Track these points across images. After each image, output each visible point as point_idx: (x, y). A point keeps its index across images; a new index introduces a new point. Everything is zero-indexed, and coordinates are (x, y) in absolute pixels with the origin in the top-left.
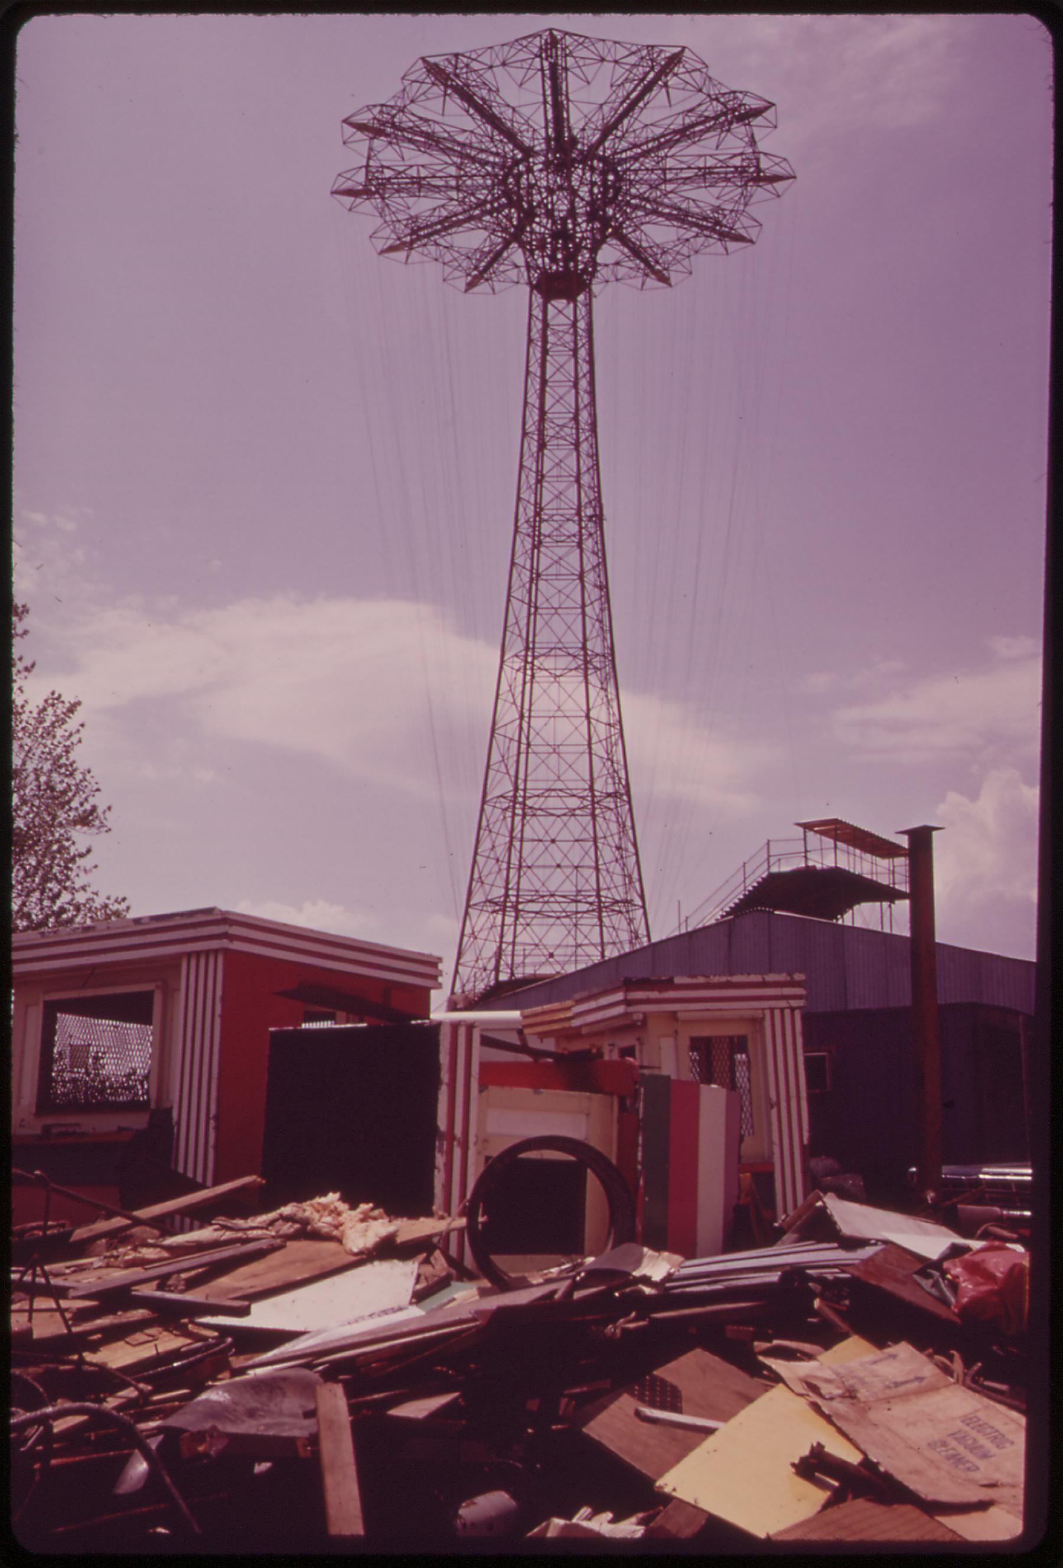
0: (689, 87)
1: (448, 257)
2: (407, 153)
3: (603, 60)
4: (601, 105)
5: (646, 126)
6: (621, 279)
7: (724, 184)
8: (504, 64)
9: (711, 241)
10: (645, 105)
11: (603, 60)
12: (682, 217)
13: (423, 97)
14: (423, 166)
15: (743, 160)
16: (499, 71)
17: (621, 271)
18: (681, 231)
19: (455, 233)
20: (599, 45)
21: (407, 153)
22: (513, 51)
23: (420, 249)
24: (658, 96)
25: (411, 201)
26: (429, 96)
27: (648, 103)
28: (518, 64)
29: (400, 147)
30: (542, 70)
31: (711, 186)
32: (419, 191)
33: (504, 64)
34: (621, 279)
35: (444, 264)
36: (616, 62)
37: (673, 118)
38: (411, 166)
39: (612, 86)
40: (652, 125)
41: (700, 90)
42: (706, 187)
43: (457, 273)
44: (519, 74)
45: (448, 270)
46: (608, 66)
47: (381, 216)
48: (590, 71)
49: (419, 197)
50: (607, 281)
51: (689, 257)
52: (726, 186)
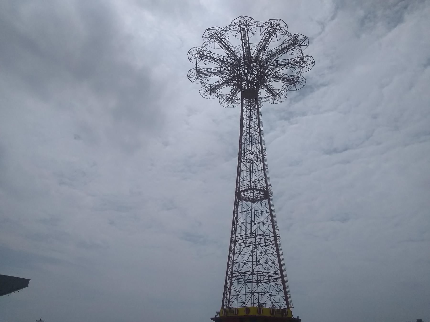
0: (282, 33)
1: (220, 97)
2: (207, 62)
3: (257, 26)
4: (259, 44)
5: (271, 50)
7: (295, 66)
8: (230, 30)
9: (292, 87)
10: (270, 41)
11: (257, 26)
12: (284, 79)
14: (211, 68)
15: (299, 60)
17: (267, 99)
19: (221, 88)
20: (257, 23)
21: (207, 62)
23: (213, 95)
24: (274, 38)
25: (209, 78)
27: (271, 40)
29: (204, 60)
30: (240, 31)
31: (290, 68)
32: (211, 75)
33: (230, 30)
35: (220, 99)
36: (261, 26)
38: (209, 69)
39: (260, 35)
40: (273, 50)
41: (286, 34)
42: (289, 68)
43: (224, 102)
44: (235, 33)
45: (221, 101)
48: (254, 30)
49: (211, 77)
50: (264, 102)
51: (286, 92)
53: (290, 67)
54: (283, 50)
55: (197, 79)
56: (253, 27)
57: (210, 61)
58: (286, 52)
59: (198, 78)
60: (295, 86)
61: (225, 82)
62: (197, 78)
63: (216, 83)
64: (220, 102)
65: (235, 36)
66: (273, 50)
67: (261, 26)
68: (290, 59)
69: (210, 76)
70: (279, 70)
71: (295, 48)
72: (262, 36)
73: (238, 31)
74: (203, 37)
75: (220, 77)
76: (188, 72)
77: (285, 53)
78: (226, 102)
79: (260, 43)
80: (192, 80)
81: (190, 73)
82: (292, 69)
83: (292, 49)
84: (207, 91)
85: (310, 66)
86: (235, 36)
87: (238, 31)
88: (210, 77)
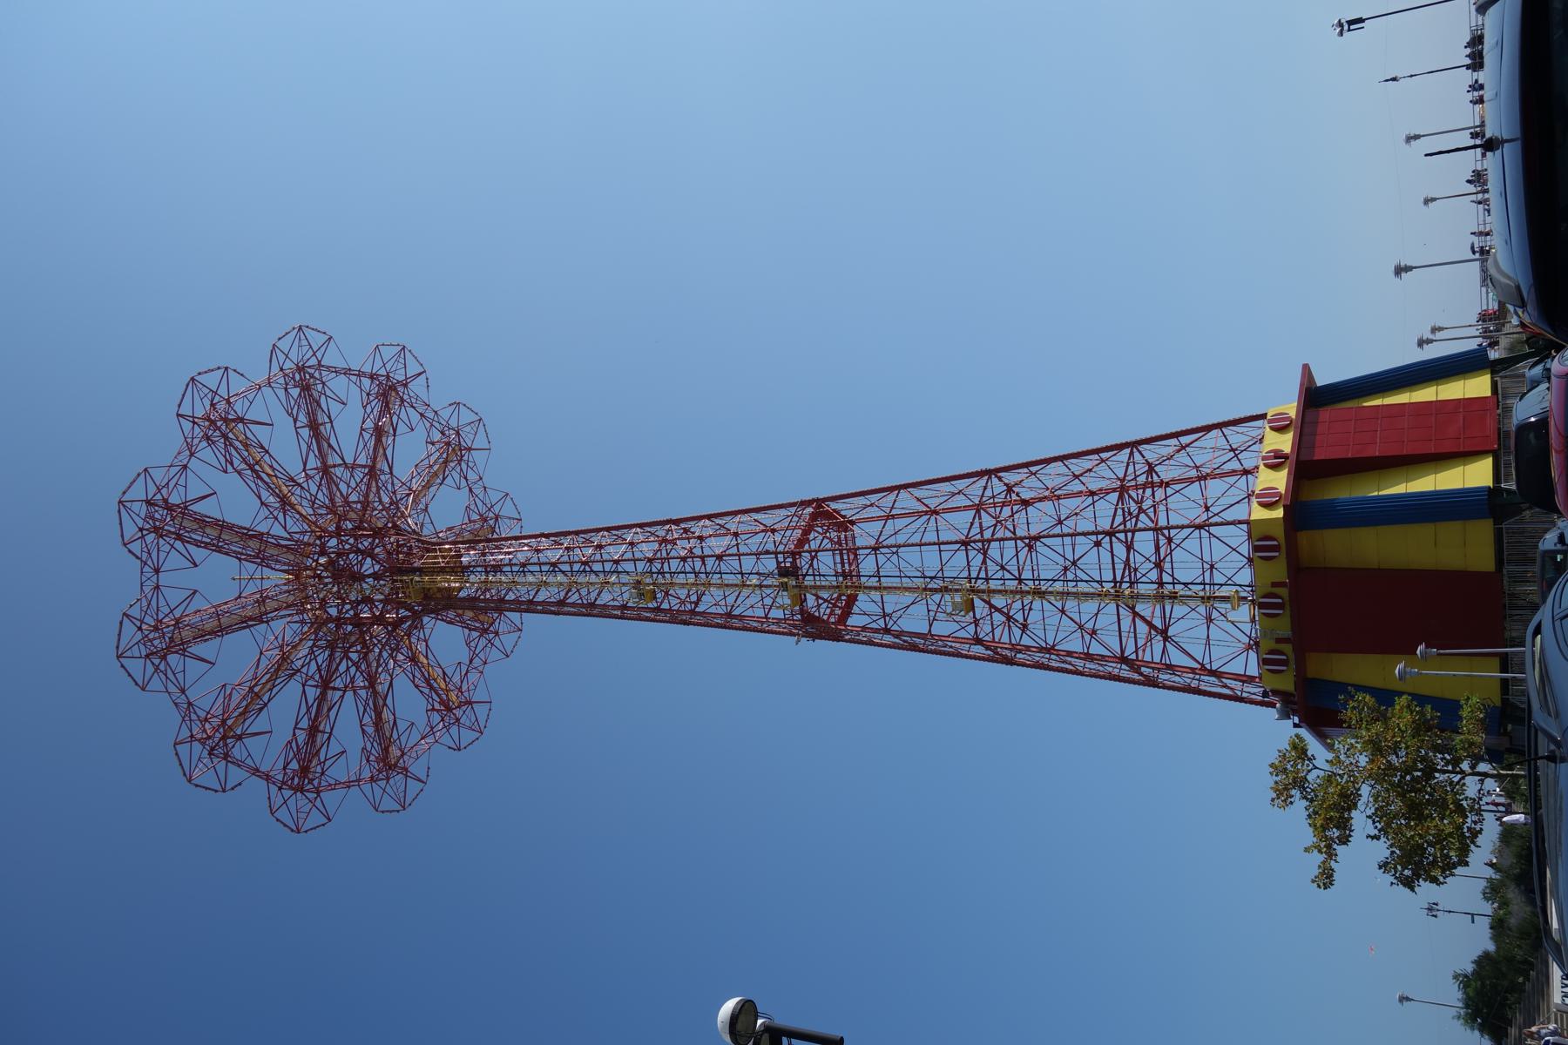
3: (185, 467)
4: (262, 503)
5: (304, 470)
11: (185, 467)
13: (180, 676)
14: (297, 724)
16: (164, 579)
18: (449, 481)
22: (149, 562)
25: (335, 748)
26: (180, 668)
28: (162, 555)
32: (324, 732)
36: (192, 454)
37: (301, 440)
39: (226, 472)
46: (193, 463)
47: (349, 787)
49: (331, 734)
52: (398, 416)
53: (391, 431)
54: (314, 426)
55: (319, 795)
56: (182, 482)
58: (329, 417)
59: (318, 793)
60: (469, 449)
61: (372, 681)
62: (311, 796)
66: (305, 464)
67: (192, 454)
68: (363, 423)
69: (326, 736)
70: (391, 468)
71: (323, 383)
73: (172, 546)
75: (342, 697)
76: (278, 820)
77: (331, 422)
78: (458, 720)
80: (316, 818)
81: (283, 814)
82: (401, 428)
83: (326, 396)
84: (388, 779)
87: (172, 546)
88: (329, 738)
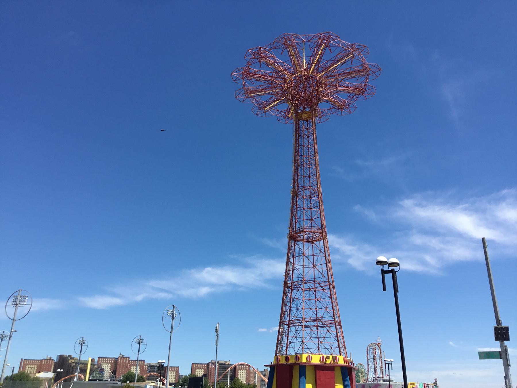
6: (334, 113)
8: (274, 48)
21: (254, 82)
34: (334, 113)
39: (310, 49)
42: (352, 78)
53: (352, 77)
57: (257, 80)
63: (270, 99)
64: (277, 119)
65: (282, 54)
72: (313, 50)
74: (245, 58)
79: (312, 55)
81: (237, 94)
84: (261, 109)
85: (377, 74)
86: (282, 54)
